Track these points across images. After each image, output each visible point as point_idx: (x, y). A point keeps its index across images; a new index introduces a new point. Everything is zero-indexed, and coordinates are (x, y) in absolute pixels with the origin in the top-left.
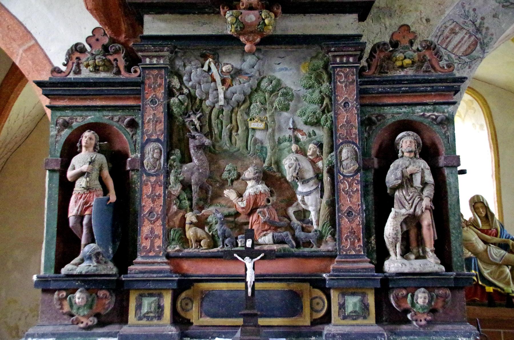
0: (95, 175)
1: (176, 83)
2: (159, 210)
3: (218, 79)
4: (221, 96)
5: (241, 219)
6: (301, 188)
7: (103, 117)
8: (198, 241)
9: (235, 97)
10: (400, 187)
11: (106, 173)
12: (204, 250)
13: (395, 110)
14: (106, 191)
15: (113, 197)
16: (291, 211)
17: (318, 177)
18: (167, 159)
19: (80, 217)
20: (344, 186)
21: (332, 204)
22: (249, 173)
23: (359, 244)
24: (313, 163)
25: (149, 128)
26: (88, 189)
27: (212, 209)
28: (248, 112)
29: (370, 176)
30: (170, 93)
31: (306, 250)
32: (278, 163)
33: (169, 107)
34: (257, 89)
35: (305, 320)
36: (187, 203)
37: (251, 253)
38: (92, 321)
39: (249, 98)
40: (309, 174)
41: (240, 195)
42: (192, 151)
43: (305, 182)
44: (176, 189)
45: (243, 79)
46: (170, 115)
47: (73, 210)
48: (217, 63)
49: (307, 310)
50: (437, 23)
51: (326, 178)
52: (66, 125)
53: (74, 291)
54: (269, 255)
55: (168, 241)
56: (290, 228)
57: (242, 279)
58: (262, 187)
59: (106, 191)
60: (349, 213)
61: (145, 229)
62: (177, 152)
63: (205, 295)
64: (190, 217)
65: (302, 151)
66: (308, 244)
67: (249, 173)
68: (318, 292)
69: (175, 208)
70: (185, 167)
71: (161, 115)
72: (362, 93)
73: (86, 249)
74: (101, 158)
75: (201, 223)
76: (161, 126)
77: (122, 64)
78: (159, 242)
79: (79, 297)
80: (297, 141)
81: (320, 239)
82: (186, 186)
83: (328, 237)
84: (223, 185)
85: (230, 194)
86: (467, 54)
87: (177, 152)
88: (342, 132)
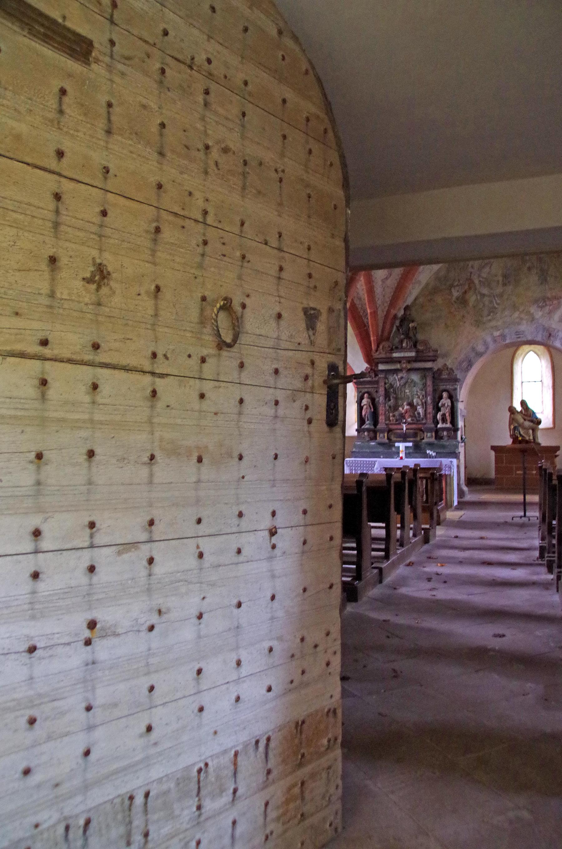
0: (368, 404)
1: (387, 381)
2: (383, 413)
3: (397, 380)
4: (398, 384)
5: (404, 415)
6: (418, 407)
7: (370, 390)
8: (393, 420)
9: (402, 384)
10: (442, 406)
11: (371, 404)
12: (394, 422)
13: (442, 387)
14: (371, 409)
15: (372, 410)
16: (416, 413)
17: (422, 404)
18: (385, 400)
19: (365, 415)
20: (428, 407)
21: (425, 411)
22: (405, 403)
23: (432, 421)
24: (421, 401)
25: (380, 393)
26: (367, 408)
27: (396, 412)
28: (405, 387)
29: (436, 403)
30: (385, 384)
31: (419, 422)
32: (413, 401)
33: (385, 387)
34: (407, 382)
35: (418, 439)
36: (390, 411)
37: (405, 423)
38: (369, 439)
39: (405, 384)
40: (420, 403)
41: (403, 409)
42: (391, 398)
43: (419, 405)
44: (387, 408)
45: (403, 379)
46: (385, 389)
47: (363, 413)
48: (397, 376)
49: (419, 436)
50: (459, 359)
51: (424, 404)
52: (361, 392)
53: (365, 432)
54: (409, 424)
55: (386, 421)
56: (415, 417)
57: (403, 429)
58: (408, 407)
59: (371, 409)
60: (429, 413)
61: (380, 418)
62: (388, 398)
63: (395, 434)
64: (391, 414)
65: (419, 397)
66: (419, 421)
67: (405, 403)
68: (421, 432)
69: (387, 412)
70: (389, 403)
71: (383, 389)
72: (433, 382)
73: (367, 422)
74: (369, 400)
75: (394, 416)
76: (383, 392)
77: (373, 376)
78: (383, 421)
79: (366, 433)
80: (417, 395)
81: (423, 419)
82: (390, 407)
83: (425, 419)
84: (399, 406)
85: (401, 409)
86: (467, 368)
87: (388, 398)
88: (428, 393)
